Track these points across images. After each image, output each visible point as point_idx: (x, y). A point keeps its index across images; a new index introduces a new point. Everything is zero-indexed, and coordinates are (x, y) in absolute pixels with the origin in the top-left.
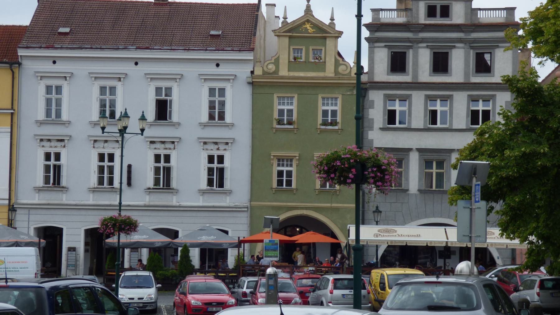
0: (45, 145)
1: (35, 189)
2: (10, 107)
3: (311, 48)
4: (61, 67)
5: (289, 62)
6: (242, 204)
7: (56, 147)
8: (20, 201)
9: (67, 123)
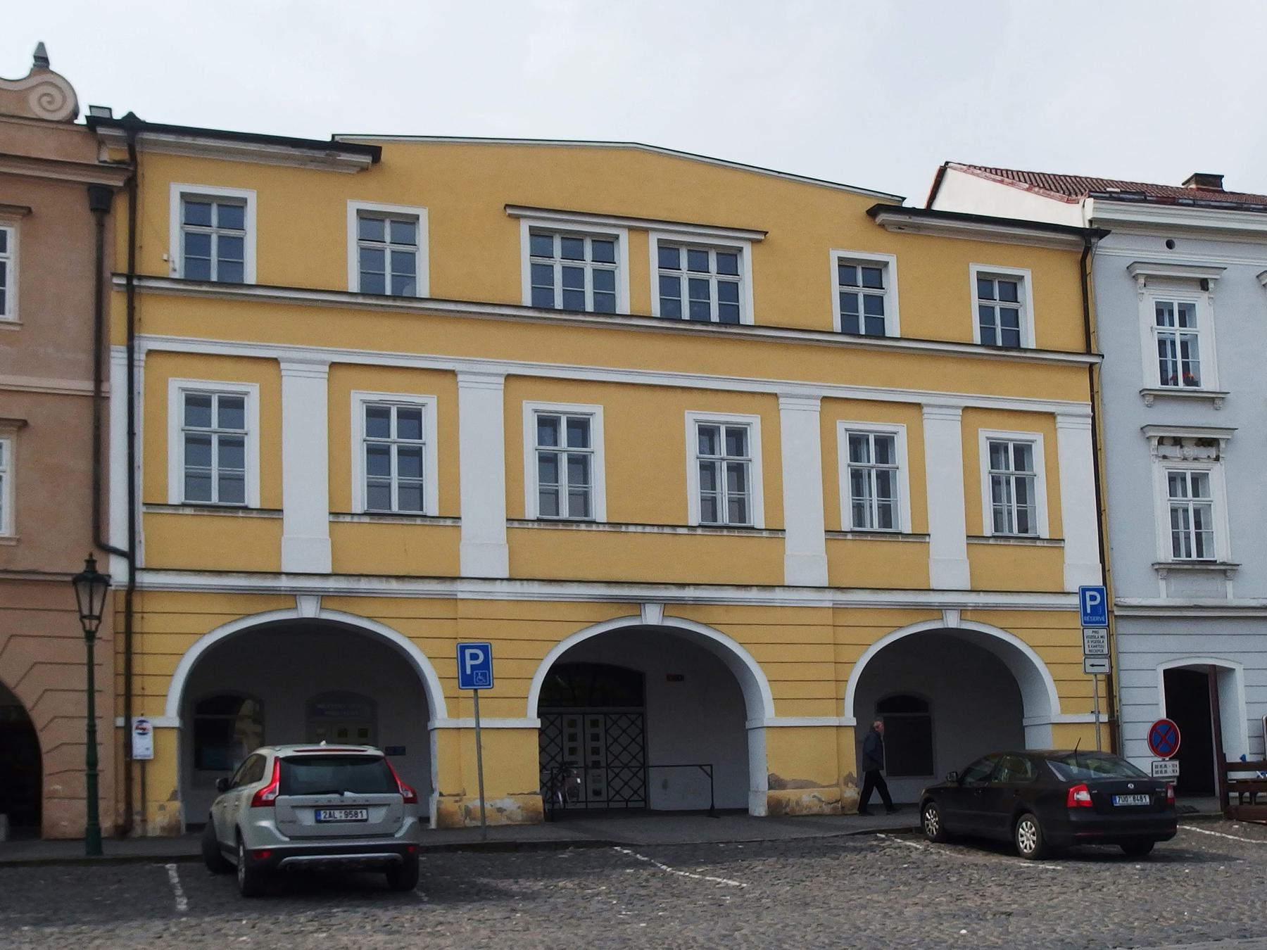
1: (1157, 567)
2: (1079, 345)
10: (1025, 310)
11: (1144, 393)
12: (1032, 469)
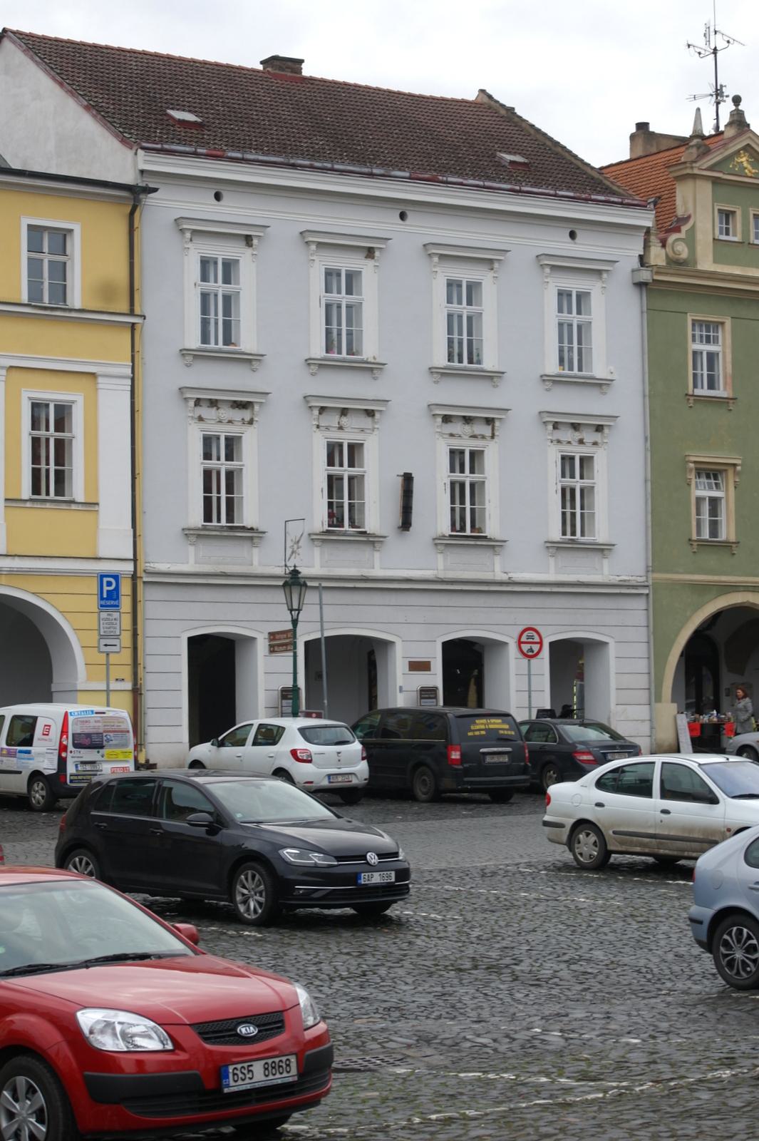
0: (203, 416)
3: (751, 213)
4: (235, 210)
5: (714, 239)
6: (633, 578)
7: (230, 422)
8: (152, 565)
9: (249, 360)
10: (73, 262)
11: (184, 353)
12: (70, 431)
